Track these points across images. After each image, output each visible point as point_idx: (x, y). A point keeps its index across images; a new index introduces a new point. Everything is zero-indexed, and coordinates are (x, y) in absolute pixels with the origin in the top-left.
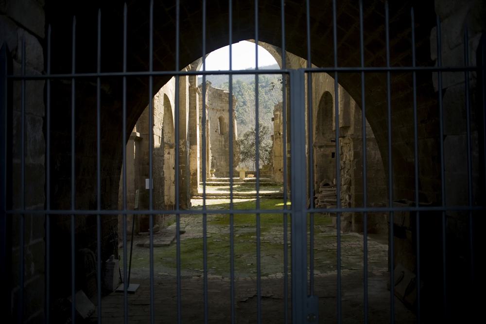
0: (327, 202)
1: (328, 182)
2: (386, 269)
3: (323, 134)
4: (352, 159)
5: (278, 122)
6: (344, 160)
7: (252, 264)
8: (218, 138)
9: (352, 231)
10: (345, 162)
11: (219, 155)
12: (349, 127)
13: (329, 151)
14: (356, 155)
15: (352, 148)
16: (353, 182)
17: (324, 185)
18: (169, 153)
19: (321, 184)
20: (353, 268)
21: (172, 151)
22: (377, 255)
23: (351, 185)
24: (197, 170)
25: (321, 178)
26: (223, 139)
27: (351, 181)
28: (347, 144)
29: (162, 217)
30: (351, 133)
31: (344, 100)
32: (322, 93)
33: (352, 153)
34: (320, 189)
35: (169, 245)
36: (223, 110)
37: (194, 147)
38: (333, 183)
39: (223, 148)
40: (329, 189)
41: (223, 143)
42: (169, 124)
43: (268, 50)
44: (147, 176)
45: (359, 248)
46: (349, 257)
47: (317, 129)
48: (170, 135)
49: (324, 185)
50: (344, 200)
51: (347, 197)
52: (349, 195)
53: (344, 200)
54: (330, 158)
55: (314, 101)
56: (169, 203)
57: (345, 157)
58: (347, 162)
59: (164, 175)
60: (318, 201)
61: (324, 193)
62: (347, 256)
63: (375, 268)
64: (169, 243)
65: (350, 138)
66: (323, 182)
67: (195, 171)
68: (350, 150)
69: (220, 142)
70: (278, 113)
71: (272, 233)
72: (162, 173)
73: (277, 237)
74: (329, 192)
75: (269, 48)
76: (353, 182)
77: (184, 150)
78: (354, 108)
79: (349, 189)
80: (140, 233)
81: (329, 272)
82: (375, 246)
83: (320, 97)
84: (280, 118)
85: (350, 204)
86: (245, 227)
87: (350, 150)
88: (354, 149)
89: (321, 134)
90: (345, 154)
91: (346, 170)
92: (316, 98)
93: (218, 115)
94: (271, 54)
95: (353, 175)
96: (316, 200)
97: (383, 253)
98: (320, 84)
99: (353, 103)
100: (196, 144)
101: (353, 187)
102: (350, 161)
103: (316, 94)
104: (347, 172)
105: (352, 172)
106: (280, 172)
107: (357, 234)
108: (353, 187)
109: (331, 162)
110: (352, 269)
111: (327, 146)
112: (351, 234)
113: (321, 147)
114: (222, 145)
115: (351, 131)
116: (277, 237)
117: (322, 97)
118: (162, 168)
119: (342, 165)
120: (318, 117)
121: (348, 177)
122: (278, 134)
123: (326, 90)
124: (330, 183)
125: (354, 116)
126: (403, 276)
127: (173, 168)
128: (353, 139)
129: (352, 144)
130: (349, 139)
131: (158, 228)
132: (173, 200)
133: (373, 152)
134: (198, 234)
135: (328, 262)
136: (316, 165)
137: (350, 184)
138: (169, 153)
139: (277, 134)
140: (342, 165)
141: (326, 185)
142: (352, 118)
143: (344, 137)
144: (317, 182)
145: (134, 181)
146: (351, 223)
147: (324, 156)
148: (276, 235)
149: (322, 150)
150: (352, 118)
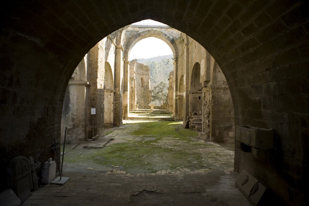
0: (196, 123)
1: (196, 113)
2: (232, 169)
3: (194, 86)
4: (211, 99)
6: (206, 100)
7: (148, 163)
9: (210, 141)
10: (206, 101)
11: (141, 98)
12: (209, 81)
13: (197, 96)
14: (213, 97)
15: (211, 93)
16: (211, 113)
17: (195, 114)
18: (110, 95)
19: (193, 113)
20: (212, 168)
21: (112, 94)
22: (225, 158)
23: (210, 115)
24: (127, 105)
25: (193, 110)
26: (143, 89)
27: (210, 112)
28: (208, 91)
29: (102, 130)
30: (210, 85)
31: (207, 66)
32: (194, 63)
33: (211, 96)
34: (192, 116)
35: (102, 148)
36: (143, 74)
37: (126, 92)
38: (199, 113)
39: (143, 94)
40: (197, 116)
41: (143, 91)
42: (110, 79)
43: (166, 42)
44: (93, 107)
45: (214, 152)
46: (208, 159)
47: (191, 83)
48: (111, 85)
49: (195, 114)
50: (205, 123)
51: (207, 121)
52: (208, 120)
53: (205, 123)
54: (198, 99)
55: (190, 68)
56: (110, 122)
57: (206, 98)
58: (208, 101)
59: (104, 106)
60: (191, 123)
61: (194, 119)
62: (207, 158)
63: (225, 168)
64: (102, 146)
65: (210, 87)
66: (194, 112)
67: (126, 105)
68: (209, 95)
70: (171, 76)
71: (164, 141)
72: (102, 106)
73: (166, 144)
74: (197, 118)
75: (167, 41)
76: (211, 113)
77: (118, 93)
78: (212, 70)
79: (208, 117)
80: (87, 140)
81: (195, 170)
82: (224, 152)
83: (193, 66)
84: (172, 79)
85: (209, 125)
86: (149, 137)
87: (209, 95)
88: (212, 94)
89: (193, 86)
90: (206, 96)
91: (207, 106)
92: (191, 66)
93: (141, 77)
94: (168, 44)
95: (211, 109)
96: (190, 122)
97: (229, 156)
98: (193, 59)
99: (213, 60)
100: (127, 91)
101: (211, 116)
102: (210, 101)
103: (191, 64)
104: (207, 107)
105: (210, 107)
106: (171, 107)
107: (212, 143)
108: (211, 116)
109: (198, 102)
110: (211, 169)
111: (196, 93)
112: (209, 143)
113: (193, 93)
115: (210, 83)
116: (166, 144)
117: (194, 66)
118: (103, 102)
119: (205, 103)
120: (192, 77)
121: (208, 110)
123: (197, 61)
124: (198, 113)
125: (212, 75)
126: (248, 180)
127: (113, 103)
128: (212, 88)
129: (211, 91)
130: (209, 88)
131: (98, 137)
132: (112, 120)
133: (223, 96)
134: (121, 141)
135: (196, 162)
136: (190, 103)
137: (209, 114)
138: (110, 95)
140: (205, 103)
141: (196, 114)
142: (211, 76)
143: (206, 87)
144: (190, 112)
145: (85, 109)
146: (209, 136)
147: (195, 98)
148: (166, 142)
149: (194, 95)
150: (211, 76)
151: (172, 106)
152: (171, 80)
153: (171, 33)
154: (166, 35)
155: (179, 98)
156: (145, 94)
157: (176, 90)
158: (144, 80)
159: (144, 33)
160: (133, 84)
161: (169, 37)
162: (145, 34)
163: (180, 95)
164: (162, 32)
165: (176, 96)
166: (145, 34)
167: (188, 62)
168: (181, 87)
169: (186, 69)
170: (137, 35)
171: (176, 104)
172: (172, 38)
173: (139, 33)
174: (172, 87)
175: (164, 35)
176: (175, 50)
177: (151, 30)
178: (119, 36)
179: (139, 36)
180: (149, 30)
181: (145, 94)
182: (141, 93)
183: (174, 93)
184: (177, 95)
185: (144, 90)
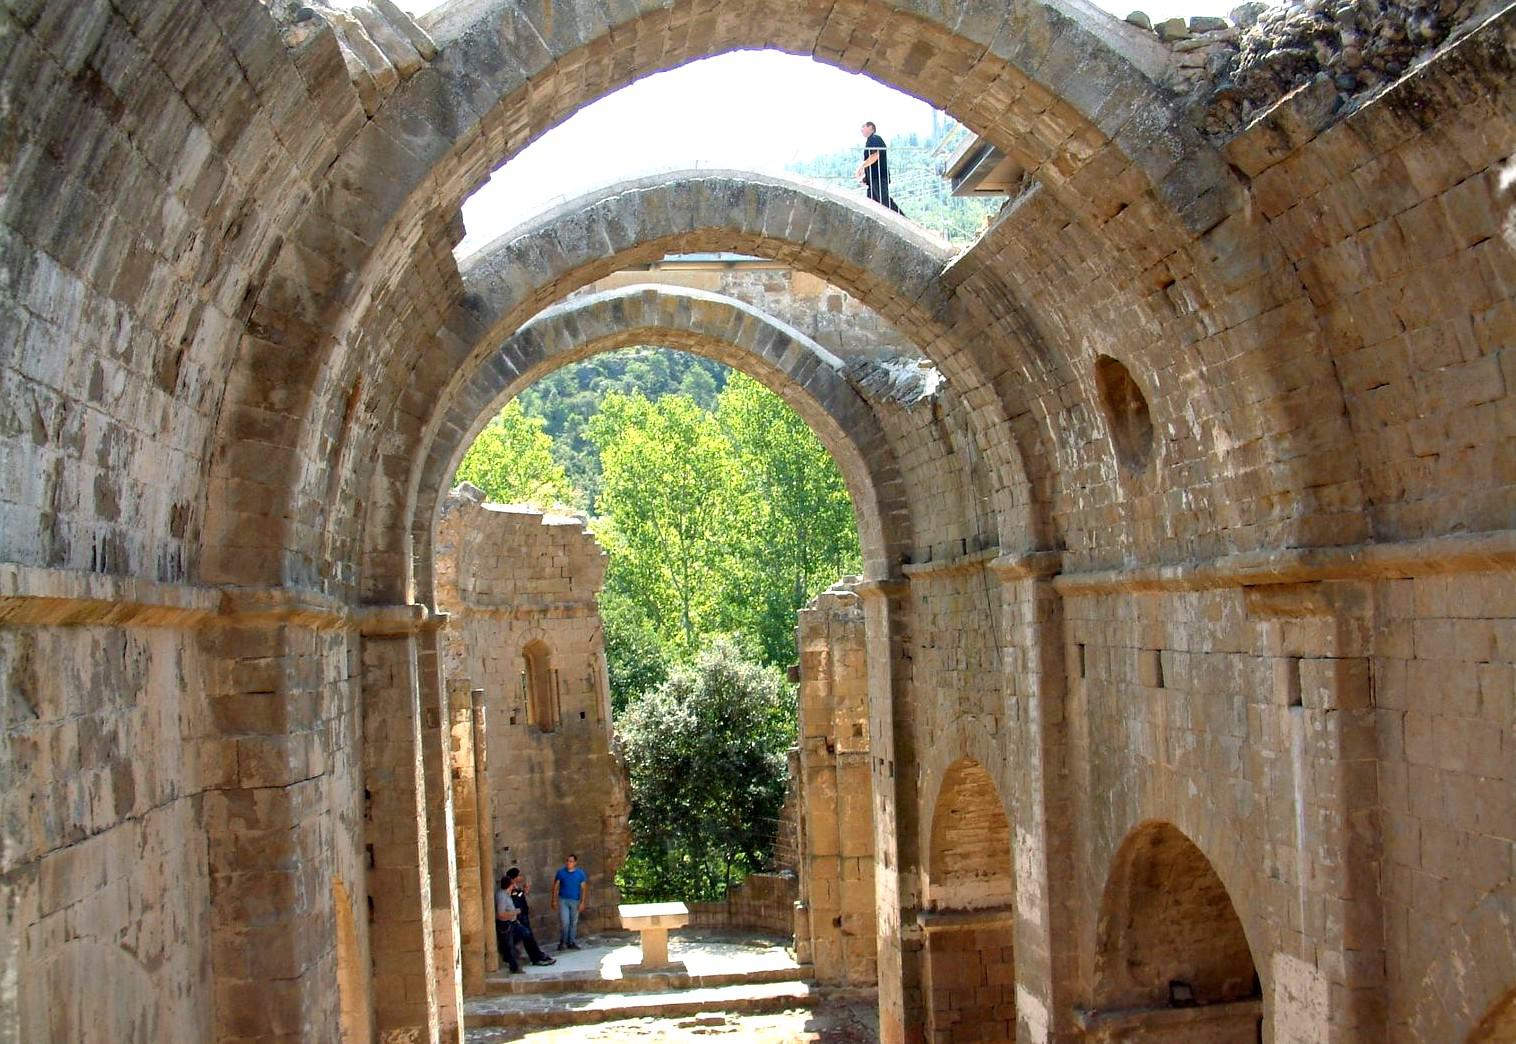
3: (1132, 964)
5: (823, 693)
8: (526, 752)
26: (549, 754)
36: (544, 611)
39: (551, 798)
41: (550, 773)
47: (1106, 947)
69: (532, 770)
84: (830, 674)
89: (1123, 966)
93: (520, 636)
106: (837, 932)
114: (543, 782)
122: (823, 752)
139: (815, 751)
151: (837, 922)
152: (821, 684)
153: (823, 307)
154: (783, 341)
155: (934, 937)
156: (568, 800)
157: (906, 862)
158: (556, 662)
159: (574, 333)
160: (466, 743)
161: (809, 361)
162: (583, 338)
163: (941, 905)
164: (740, 316)
165: (907, 914)
166: (583, 338)
167: (1057, 727)
168: (951, 835)
169: (1038, 797)
170: (508, 350)
171: (912, 986)
172: (837, 362)
173: (528, 331)
174: (831, 749)
175: (762, 343)
176: (877, 479)
177: (635, 301)
178: (381, 516)
179: (523, 367)
180: (617, 305)
181: (568, 800)
182: (537, 792)
183: (886, 881)
184: (919, 909)
185: (559, 764)
